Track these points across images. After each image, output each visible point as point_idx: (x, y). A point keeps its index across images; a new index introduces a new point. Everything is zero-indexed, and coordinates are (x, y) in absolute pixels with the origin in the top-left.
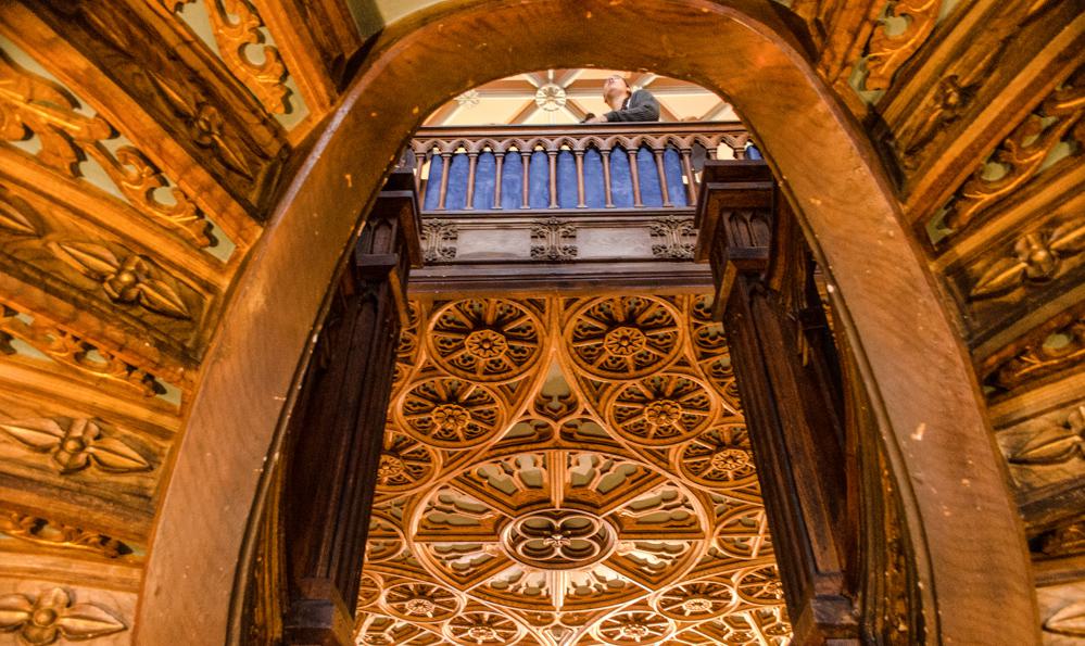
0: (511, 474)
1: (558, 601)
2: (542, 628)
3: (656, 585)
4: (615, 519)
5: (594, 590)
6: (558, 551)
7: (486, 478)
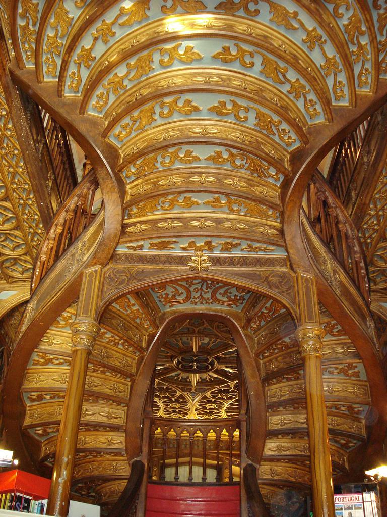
0: (179, 342)
1: (194, 383)
3: (233, 380)
4: (218, 359)
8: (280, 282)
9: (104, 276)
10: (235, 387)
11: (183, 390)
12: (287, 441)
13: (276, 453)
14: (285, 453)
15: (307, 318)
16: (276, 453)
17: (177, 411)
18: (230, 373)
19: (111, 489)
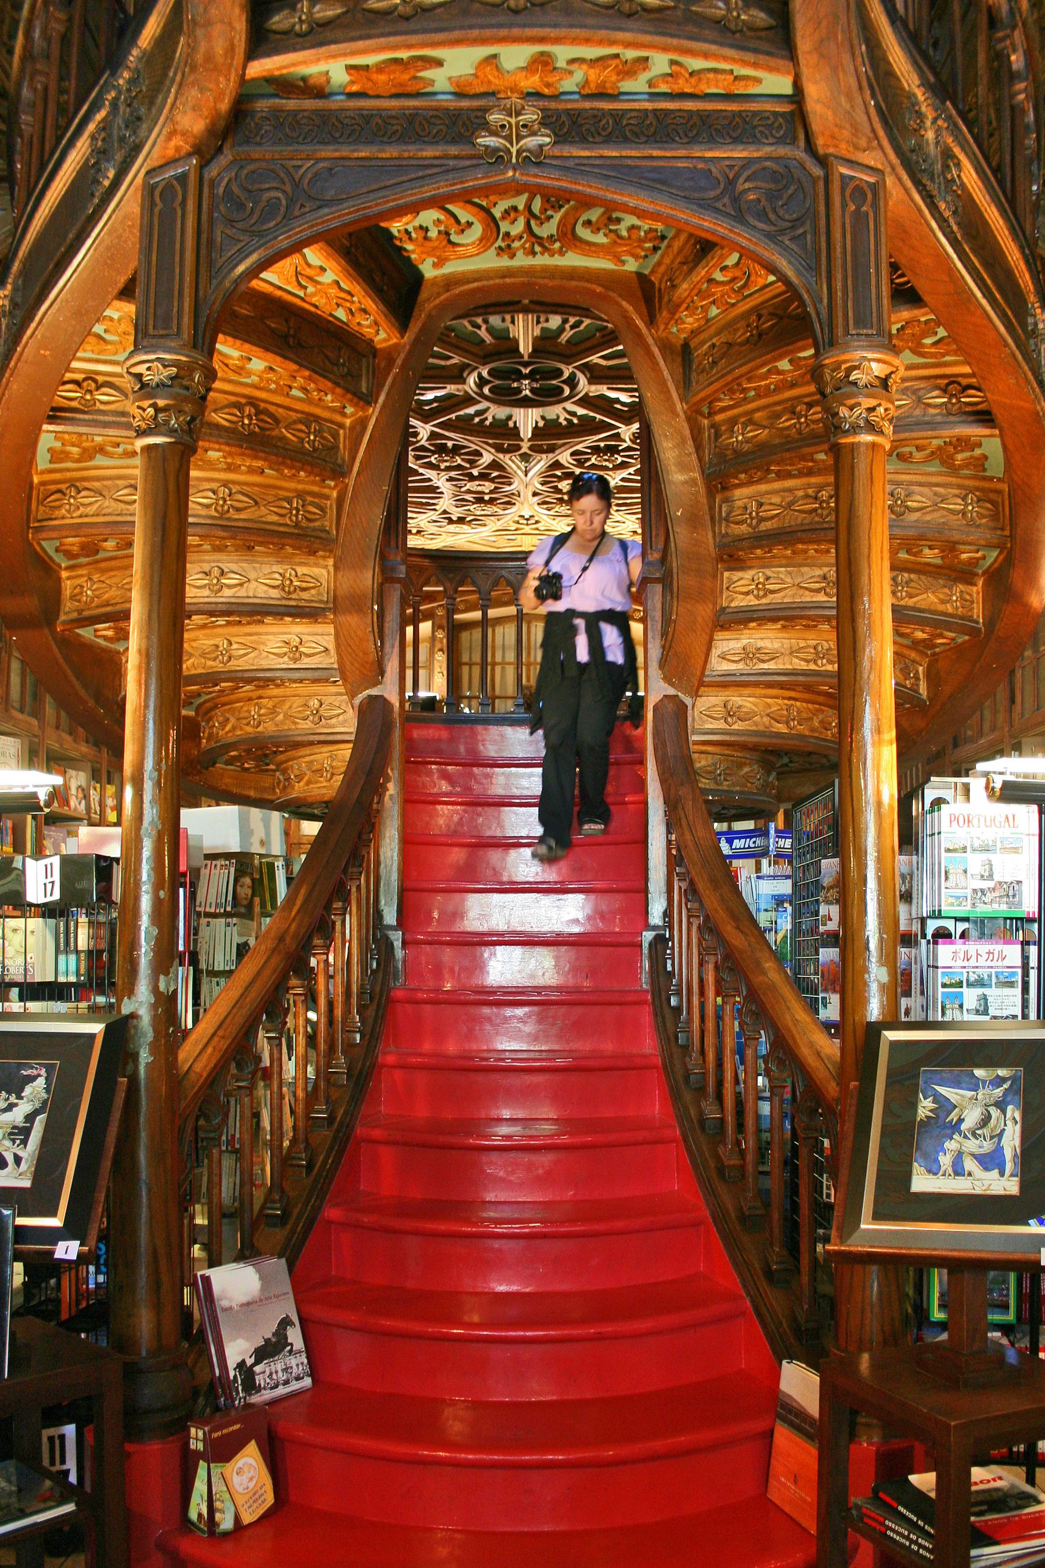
0: (479, 327)
2: (508, 456)
3: (628, 422)
4: (586, 368)
5: (564, 423)
6: (527, 392)
7: (453, 330)
8: (772, 196)
9: (212, 196)
10: (635, 437)
11: (499, 449)
12: (771, 634)
13: (741, 666)
14: (765, 666)
15: (851, 322)
16: (741, 666)
17: (487, 498)
18: (623, 404)
19: (312, 762)
